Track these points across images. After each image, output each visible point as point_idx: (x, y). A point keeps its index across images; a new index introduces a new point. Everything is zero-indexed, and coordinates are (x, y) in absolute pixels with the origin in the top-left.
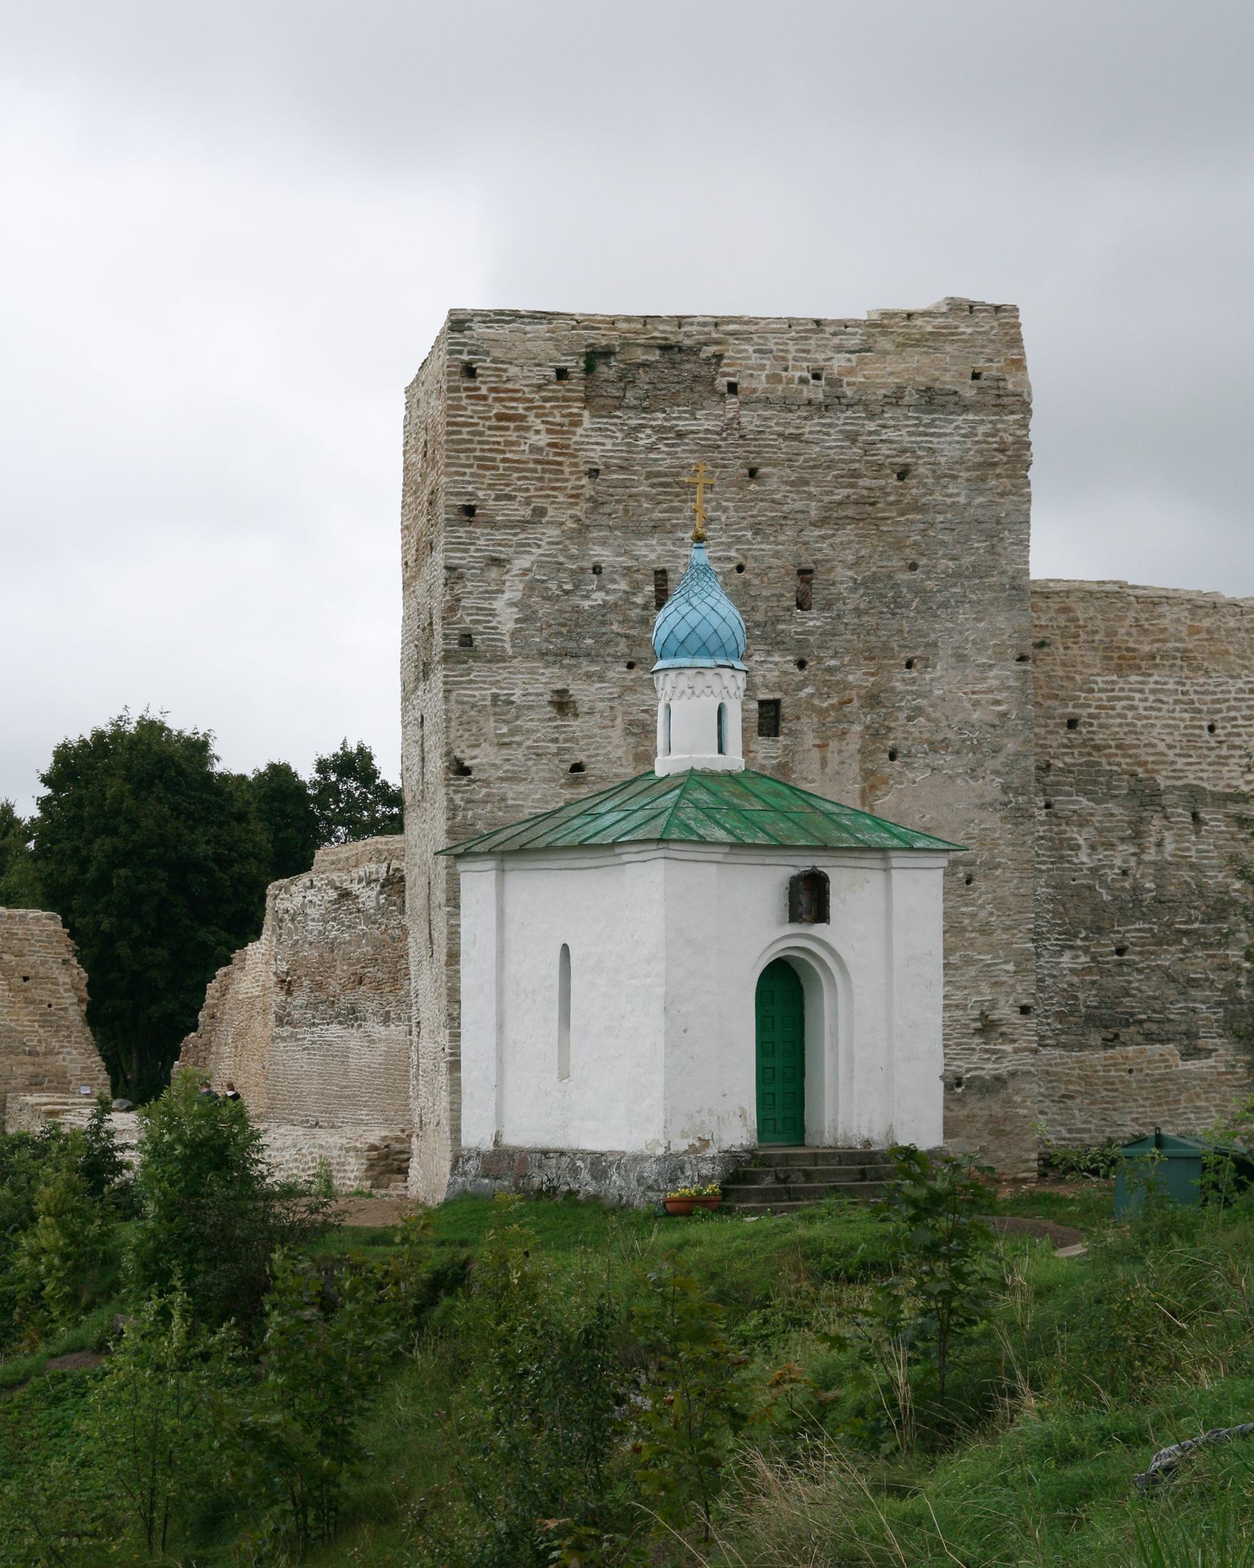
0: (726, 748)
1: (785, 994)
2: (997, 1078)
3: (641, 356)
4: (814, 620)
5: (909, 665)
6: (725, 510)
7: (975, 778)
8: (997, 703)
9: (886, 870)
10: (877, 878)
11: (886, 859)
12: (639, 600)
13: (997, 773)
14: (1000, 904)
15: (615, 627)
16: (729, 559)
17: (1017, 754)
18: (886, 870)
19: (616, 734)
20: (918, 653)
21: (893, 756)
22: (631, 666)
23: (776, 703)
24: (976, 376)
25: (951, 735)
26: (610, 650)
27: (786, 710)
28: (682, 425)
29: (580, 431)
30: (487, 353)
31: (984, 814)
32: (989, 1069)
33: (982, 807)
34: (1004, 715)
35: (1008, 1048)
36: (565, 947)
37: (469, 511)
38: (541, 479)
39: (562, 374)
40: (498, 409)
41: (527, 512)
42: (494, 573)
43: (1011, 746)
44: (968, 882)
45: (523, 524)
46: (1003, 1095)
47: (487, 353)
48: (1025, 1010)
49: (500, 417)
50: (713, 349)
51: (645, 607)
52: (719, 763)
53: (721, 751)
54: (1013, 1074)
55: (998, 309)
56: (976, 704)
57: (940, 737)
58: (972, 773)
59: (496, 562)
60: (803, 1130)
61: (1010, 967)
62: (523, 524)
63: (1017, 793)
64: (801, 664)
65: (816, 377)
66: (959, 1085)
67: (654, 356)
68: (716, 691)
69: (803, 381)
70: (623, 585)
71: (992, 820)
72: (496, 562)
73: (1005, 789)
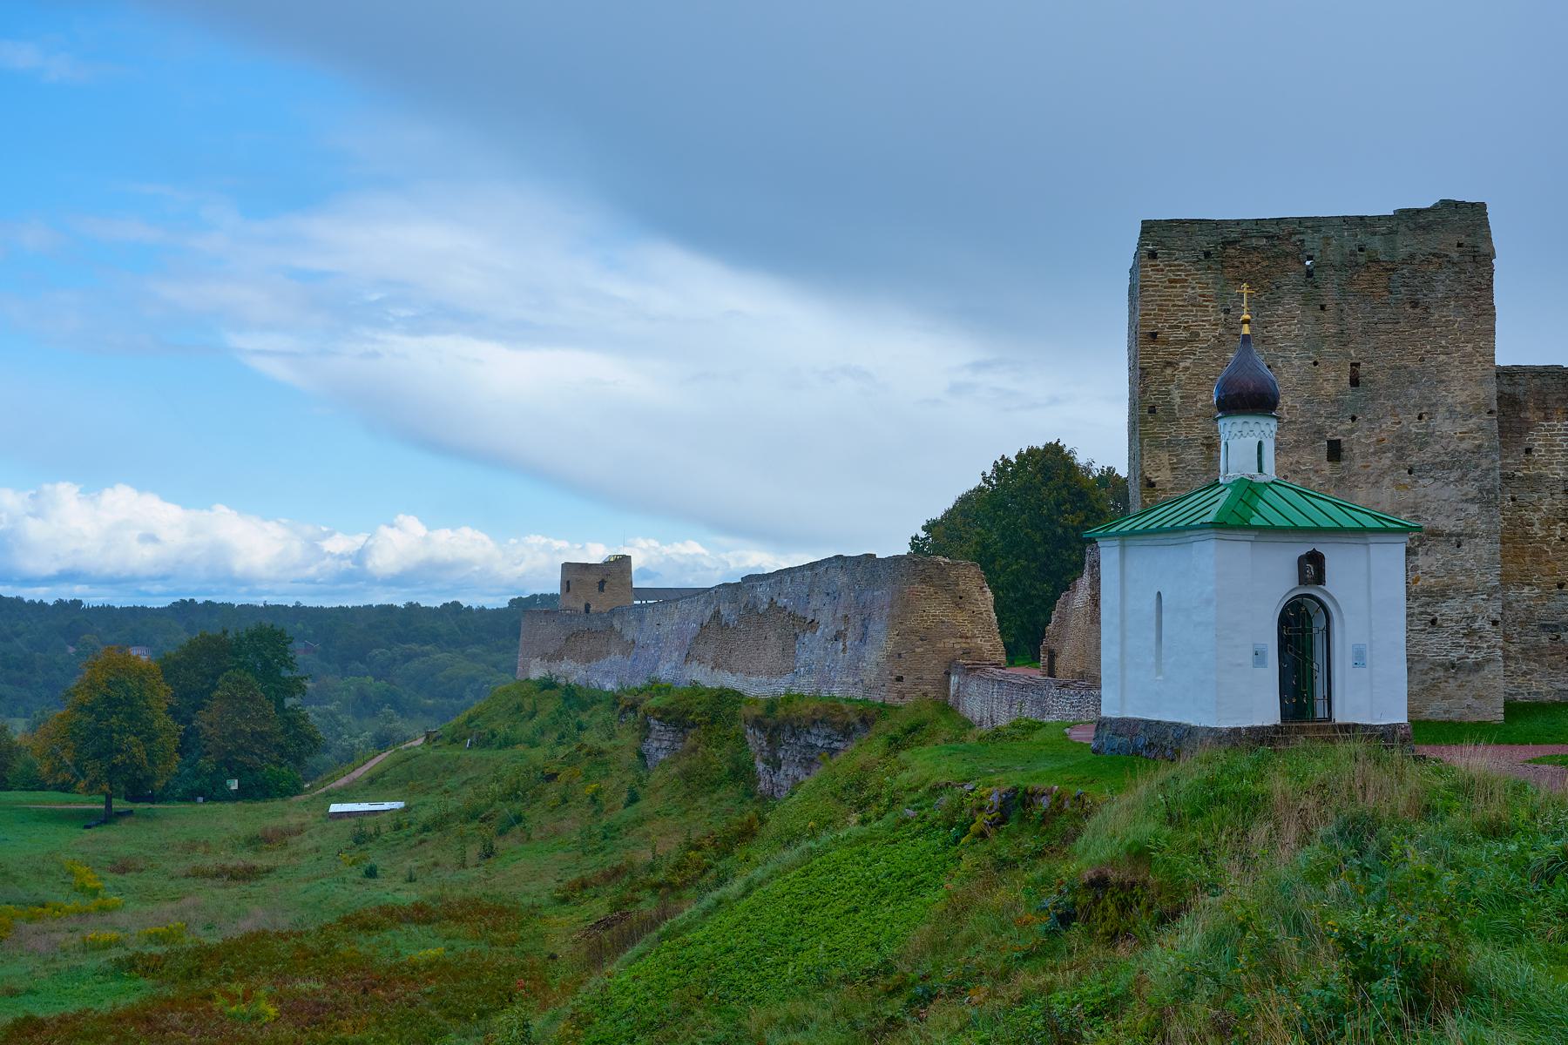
0: (1265, 470)
1: (1301, 634)
5: (1420, 417)
14: (1478, 559)
20: (1425, 409)
24: (1459, 245)
27: (1344, 446)
34: (1480, 446)
37: (1154, 335)
39: (1207, 255)
41: (1184, 335)
42: (1169, 371)
43: (1485, 464)
45: (1182, 343)
46: (1482, 673)
48: (1495, 623)
52: (1260, 479)
53: (1260, 470)
59: (1169, 364)
62: (1182, 343)
63: (1488, 492)
64: (1354, 419)
65: (1361, 250)
72: (1169, 364)
73: (1480, 491)
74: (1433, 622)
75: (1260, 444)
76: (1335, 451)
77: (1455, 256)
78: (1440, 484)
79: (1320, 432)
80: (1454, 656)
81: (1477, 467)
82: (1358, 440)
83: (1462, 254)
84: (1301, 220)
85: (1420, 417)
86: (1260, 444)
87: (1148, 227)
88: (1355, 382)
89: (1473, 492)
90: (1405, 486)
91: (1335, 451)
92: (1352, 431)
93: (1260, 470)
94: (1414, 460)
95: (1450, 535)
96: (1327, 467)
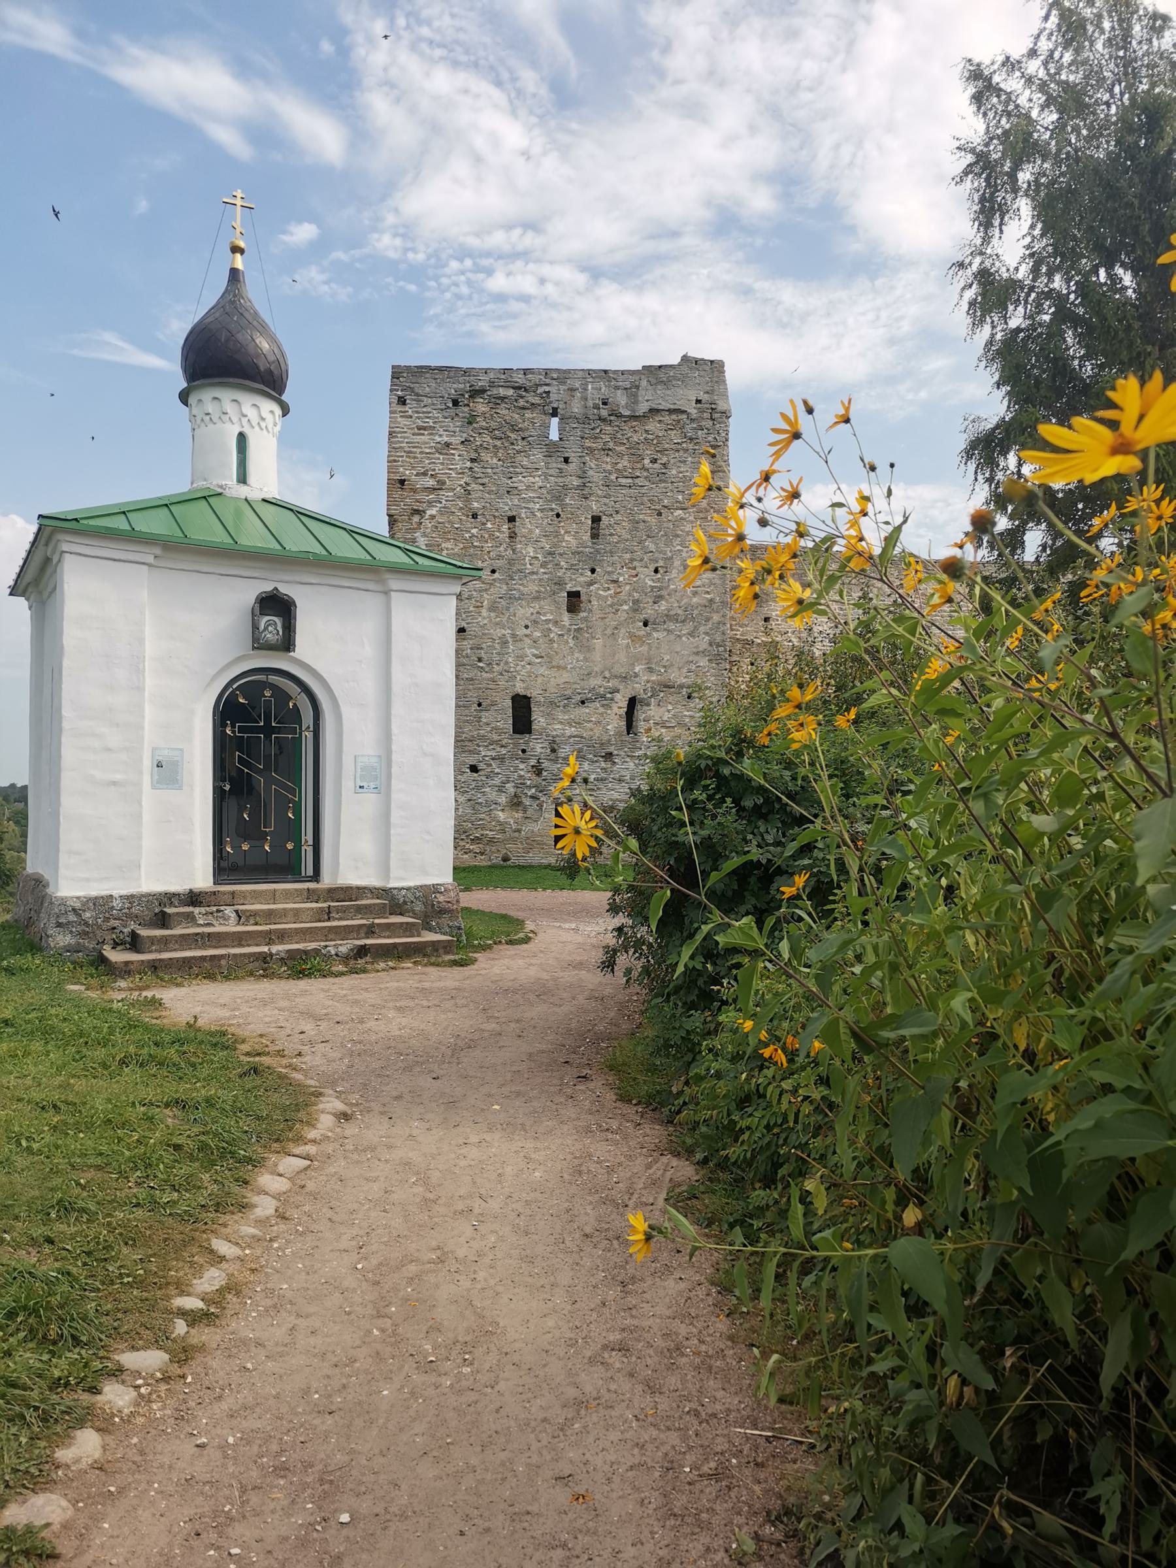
0: (252, 478)
5: (656, 571)
7: (694, 637)
8: (708, 593)
9: (386, 593)
10: (372, 602)
11: (382, 582)
13: (707, 634)
16: (552, 510)
17: (719, 623)
18: (386, 593)
19: (484, 612)
20: (661, 563)
21: (645, 624)
22: (493, 571)
23: (578, 592)
24: (698, 401)
25: (679, 612)
31: (696, 658)
33: (697, 653)
34: (711, 600)
37: (402, 482)
38: (442, 464)
42: (416, 519)
43: (716, 618)
50: (547, 389)
52: (243, 491)
55: (712, 362)
56: (695, 594)
57: (672, 613)
58: (691, 634)
63: (718, 646)
64: (593, 571)
65: (605, 404)
67: (510, 392)
68: (235, 419)
69: (596, 407)
71: (703, 662)
75: (242, 437)
76: (574, 601)
77: (693, 412)
78: (672, 637)
79: (560, 583)
81: (707, 620)
82: (598, 595)
83: (701, 411)
84: (547, 372)
85: (656, 571)
86: (242, 437)
87: (397, 373)
89: (704, 645)
90: (640, 638)
91: (574, 601)
92: (591, 584)
93: (243, 479)
94: (649, 612)
95: (681, 686)
96: (566, 618)
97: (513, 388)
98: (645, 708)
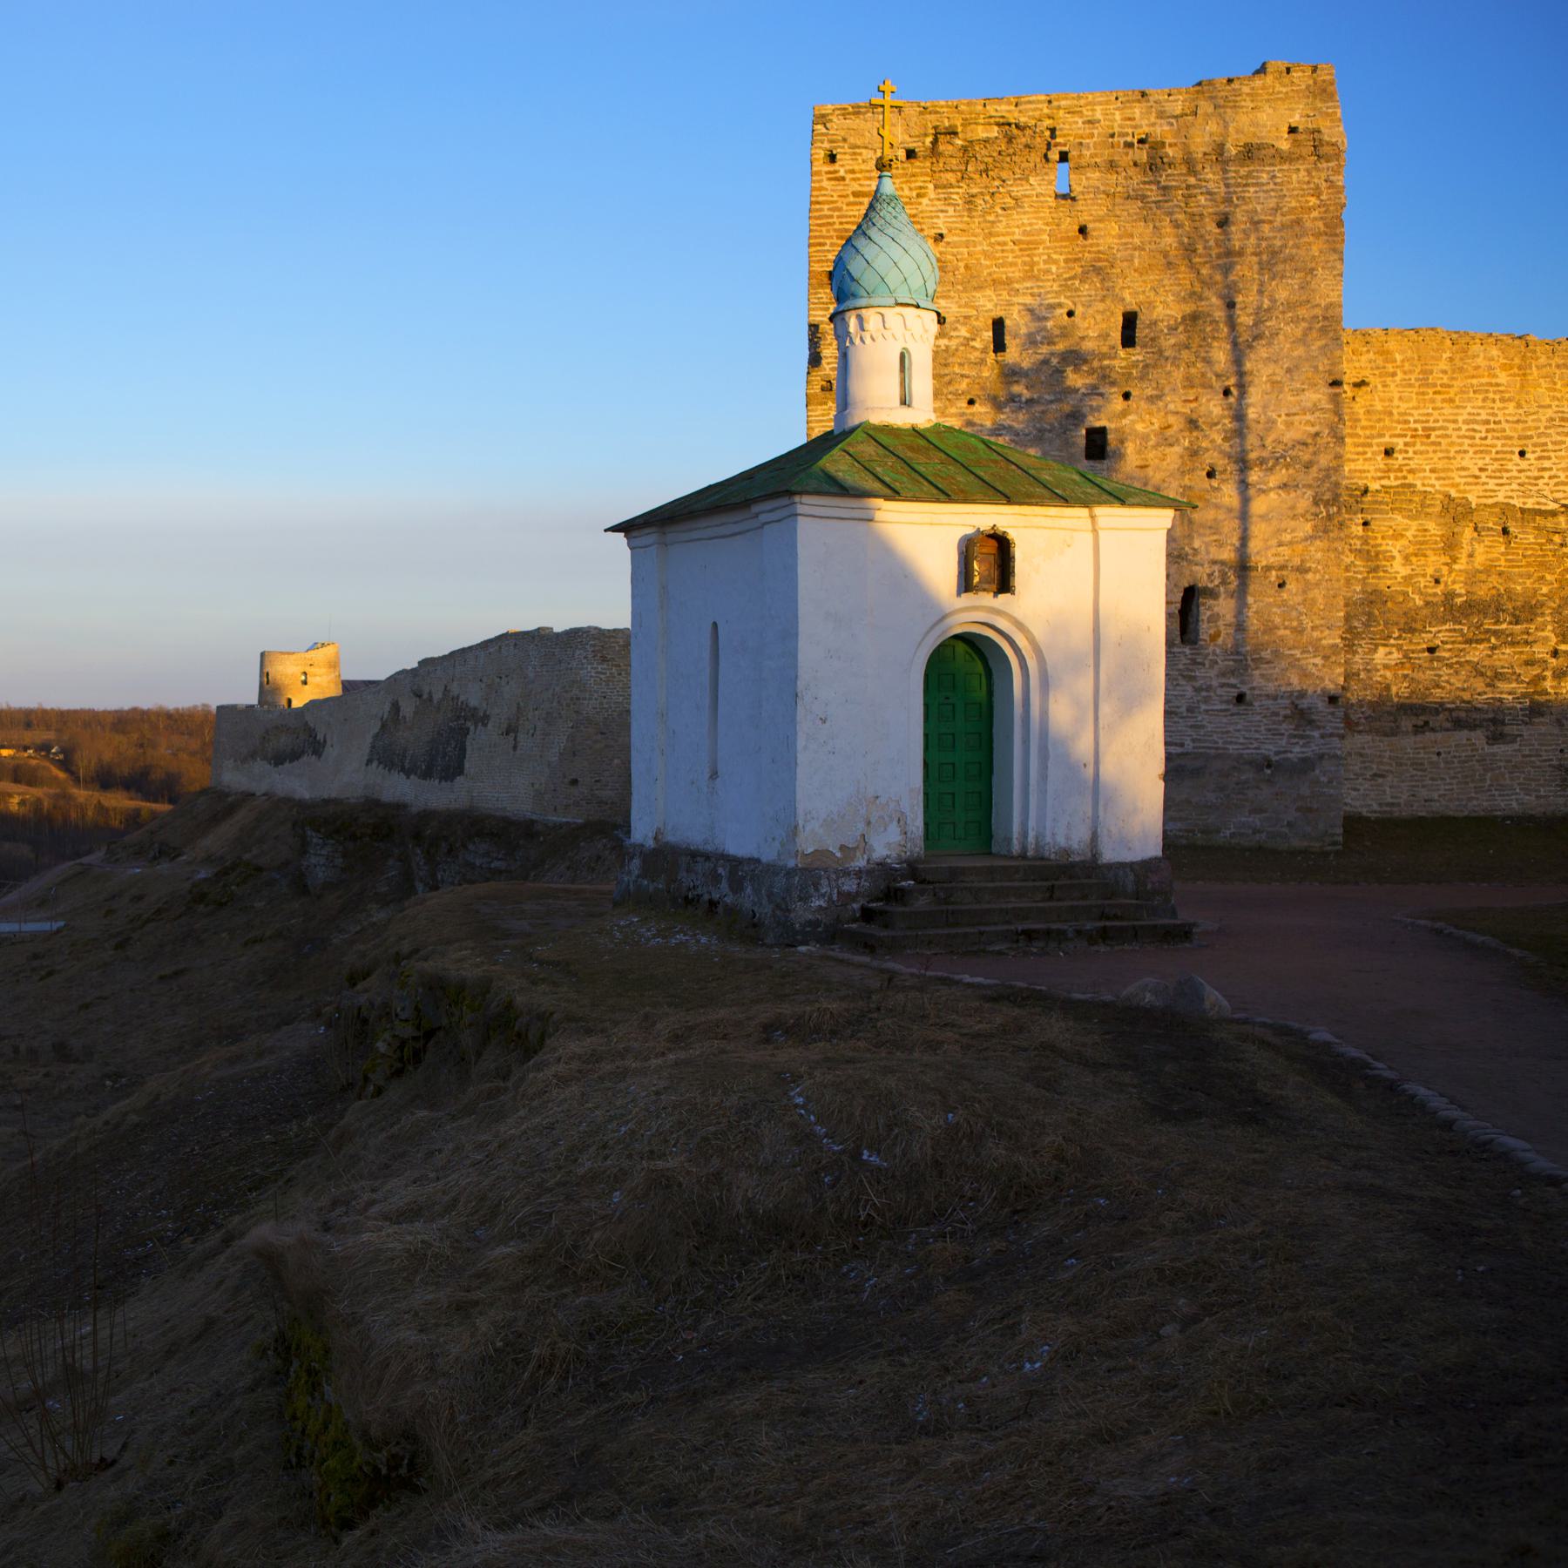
2: (1304, 760)
3: (981, 133)
4: (1137, 355)
6: (1056, 262)
12: (977, 344)
13: (1309, 486)
15: (957, 369)
22: (971, 402)
26: (951, 389)
28: (1017, 190)
29: (925, 201)
30: (845, 140)
31: (1293, 523)
32: (1297, 752)
33: (1294, 517)
35: (1316, 734)
36: (715, 624)
40: (856, 187)
44: (1280, 586)
47: (845, 140)
49: (855, 194)
51: (984, 351)
54: (1321, 757)
60: (991, 837)
61: (1318, 661)
66: (1269, 766)
67: (994, 132)
69: (1129, 145)
70: (964, 332)
73: (1316, 503)
74: (1240, 698)
80: (1269, 749)
88: (1128, 340)
92: (1124, 414)
97: (998, 124)
98: (1210, 602)
